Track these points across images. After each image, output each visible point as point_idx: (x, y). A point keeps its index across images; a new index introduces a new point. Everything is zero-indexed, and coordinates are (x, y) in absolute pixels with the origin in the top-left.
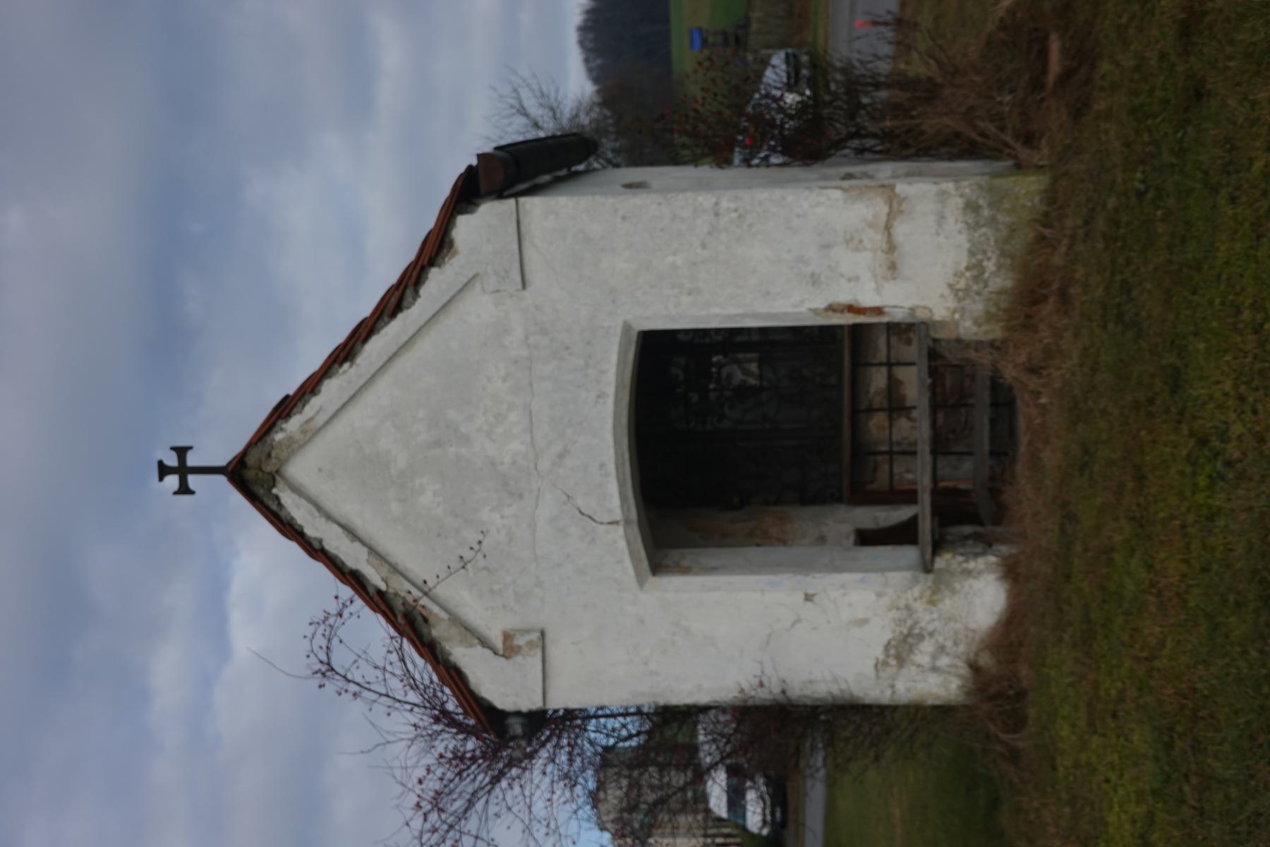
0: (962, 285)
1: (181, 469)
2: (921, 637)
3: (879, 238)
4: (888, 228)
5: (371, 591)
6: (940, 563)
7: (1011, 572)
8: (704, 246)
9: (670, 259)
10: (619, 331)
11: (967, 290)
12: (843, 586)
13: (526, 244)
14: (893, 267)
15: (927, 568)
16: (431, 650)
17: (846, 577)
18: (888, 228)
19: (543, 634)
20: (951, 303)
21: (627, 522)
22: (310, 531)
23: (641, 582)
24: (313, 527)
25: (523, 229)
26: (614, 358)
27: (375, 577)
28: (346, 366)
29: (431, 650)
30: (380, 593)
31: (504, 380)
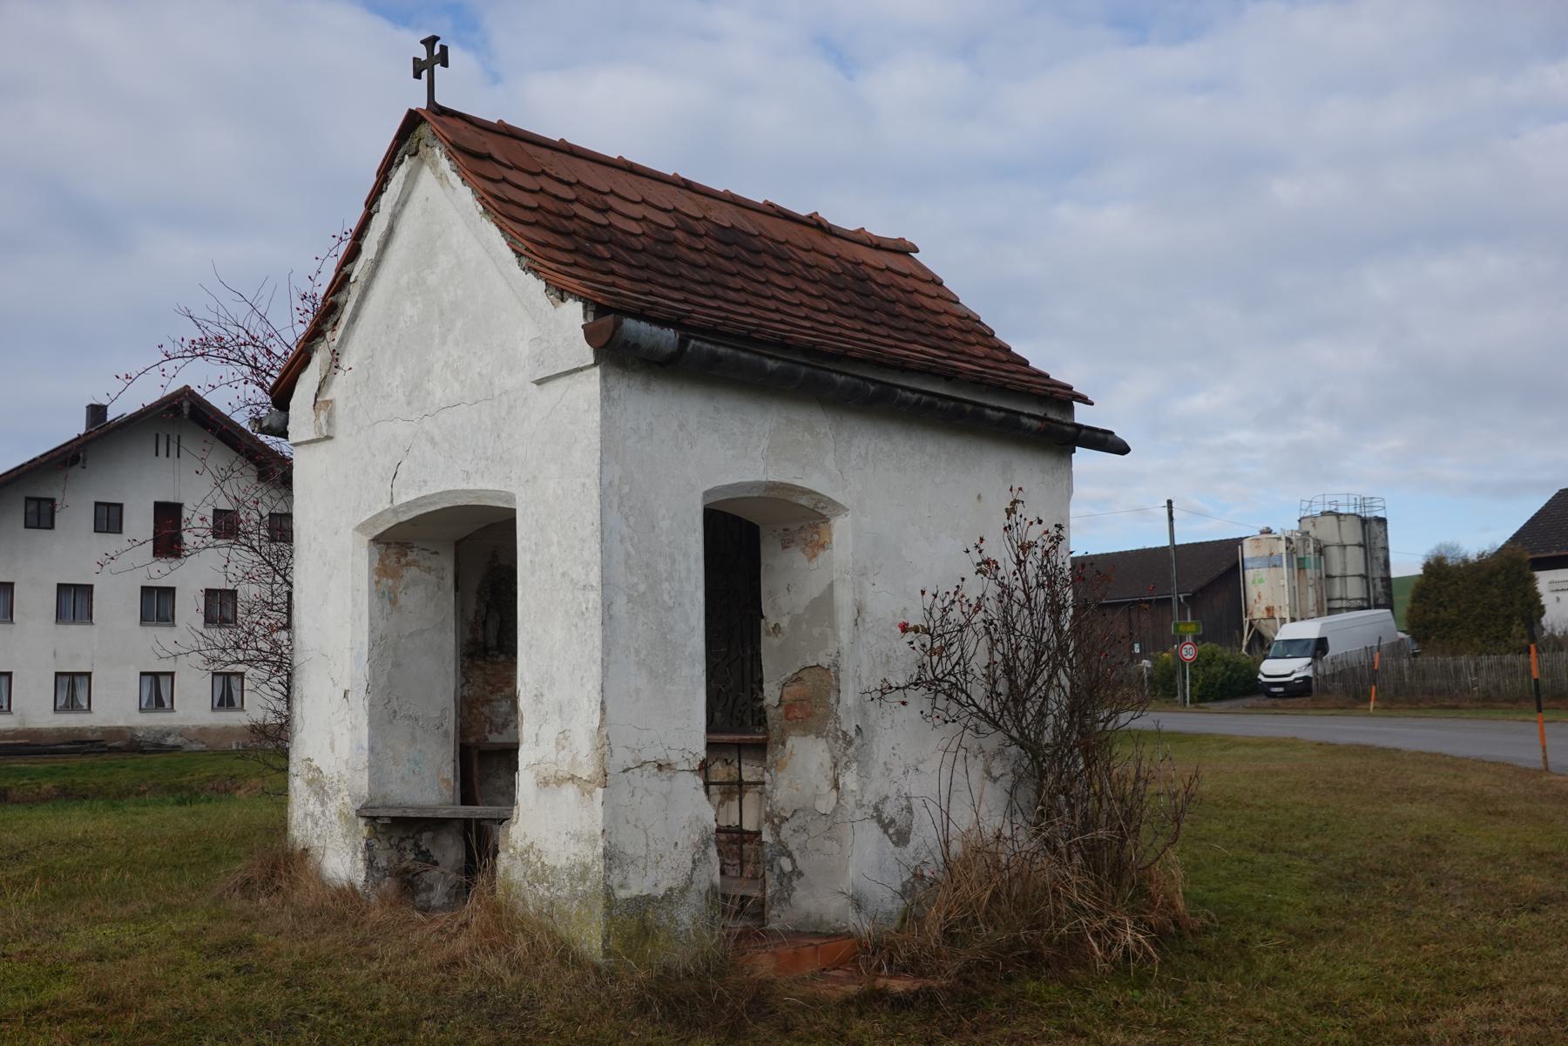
0: (533, 858)
1: (434, 57)
2: (323, 804)
3: (565, 770)
4: (572, 778)
5: (347, 269)
6: (362, 822)
7: (348, 894)
8: (563, 575)
9: (555, 539)
10: (838, 497)
11: (528, 863)
12: (354, 727)
13: (565, 381)
14: (546, 783)
15: (359, 813)
16: (315, 334)
17: (365, 731)
18: (572, 778)
19: (328, 438)
20: (520, 845)
21: (395, 511)
22: (384, 198)
23: (361, 528)
24: (387, 201)
25: (577, 376)
26: (490, 487)
27: (359, 269)
28: (480, 208)
29: (315, 334)
30: (348, 276)
31: (480, 374)
